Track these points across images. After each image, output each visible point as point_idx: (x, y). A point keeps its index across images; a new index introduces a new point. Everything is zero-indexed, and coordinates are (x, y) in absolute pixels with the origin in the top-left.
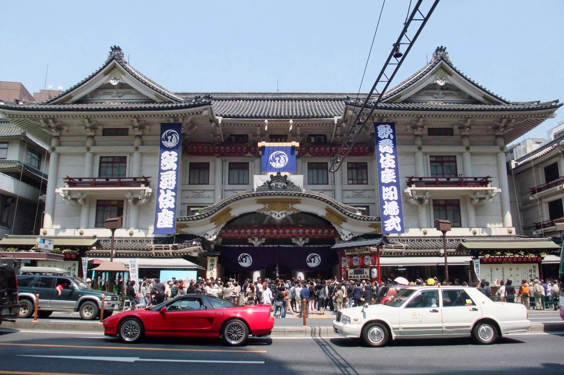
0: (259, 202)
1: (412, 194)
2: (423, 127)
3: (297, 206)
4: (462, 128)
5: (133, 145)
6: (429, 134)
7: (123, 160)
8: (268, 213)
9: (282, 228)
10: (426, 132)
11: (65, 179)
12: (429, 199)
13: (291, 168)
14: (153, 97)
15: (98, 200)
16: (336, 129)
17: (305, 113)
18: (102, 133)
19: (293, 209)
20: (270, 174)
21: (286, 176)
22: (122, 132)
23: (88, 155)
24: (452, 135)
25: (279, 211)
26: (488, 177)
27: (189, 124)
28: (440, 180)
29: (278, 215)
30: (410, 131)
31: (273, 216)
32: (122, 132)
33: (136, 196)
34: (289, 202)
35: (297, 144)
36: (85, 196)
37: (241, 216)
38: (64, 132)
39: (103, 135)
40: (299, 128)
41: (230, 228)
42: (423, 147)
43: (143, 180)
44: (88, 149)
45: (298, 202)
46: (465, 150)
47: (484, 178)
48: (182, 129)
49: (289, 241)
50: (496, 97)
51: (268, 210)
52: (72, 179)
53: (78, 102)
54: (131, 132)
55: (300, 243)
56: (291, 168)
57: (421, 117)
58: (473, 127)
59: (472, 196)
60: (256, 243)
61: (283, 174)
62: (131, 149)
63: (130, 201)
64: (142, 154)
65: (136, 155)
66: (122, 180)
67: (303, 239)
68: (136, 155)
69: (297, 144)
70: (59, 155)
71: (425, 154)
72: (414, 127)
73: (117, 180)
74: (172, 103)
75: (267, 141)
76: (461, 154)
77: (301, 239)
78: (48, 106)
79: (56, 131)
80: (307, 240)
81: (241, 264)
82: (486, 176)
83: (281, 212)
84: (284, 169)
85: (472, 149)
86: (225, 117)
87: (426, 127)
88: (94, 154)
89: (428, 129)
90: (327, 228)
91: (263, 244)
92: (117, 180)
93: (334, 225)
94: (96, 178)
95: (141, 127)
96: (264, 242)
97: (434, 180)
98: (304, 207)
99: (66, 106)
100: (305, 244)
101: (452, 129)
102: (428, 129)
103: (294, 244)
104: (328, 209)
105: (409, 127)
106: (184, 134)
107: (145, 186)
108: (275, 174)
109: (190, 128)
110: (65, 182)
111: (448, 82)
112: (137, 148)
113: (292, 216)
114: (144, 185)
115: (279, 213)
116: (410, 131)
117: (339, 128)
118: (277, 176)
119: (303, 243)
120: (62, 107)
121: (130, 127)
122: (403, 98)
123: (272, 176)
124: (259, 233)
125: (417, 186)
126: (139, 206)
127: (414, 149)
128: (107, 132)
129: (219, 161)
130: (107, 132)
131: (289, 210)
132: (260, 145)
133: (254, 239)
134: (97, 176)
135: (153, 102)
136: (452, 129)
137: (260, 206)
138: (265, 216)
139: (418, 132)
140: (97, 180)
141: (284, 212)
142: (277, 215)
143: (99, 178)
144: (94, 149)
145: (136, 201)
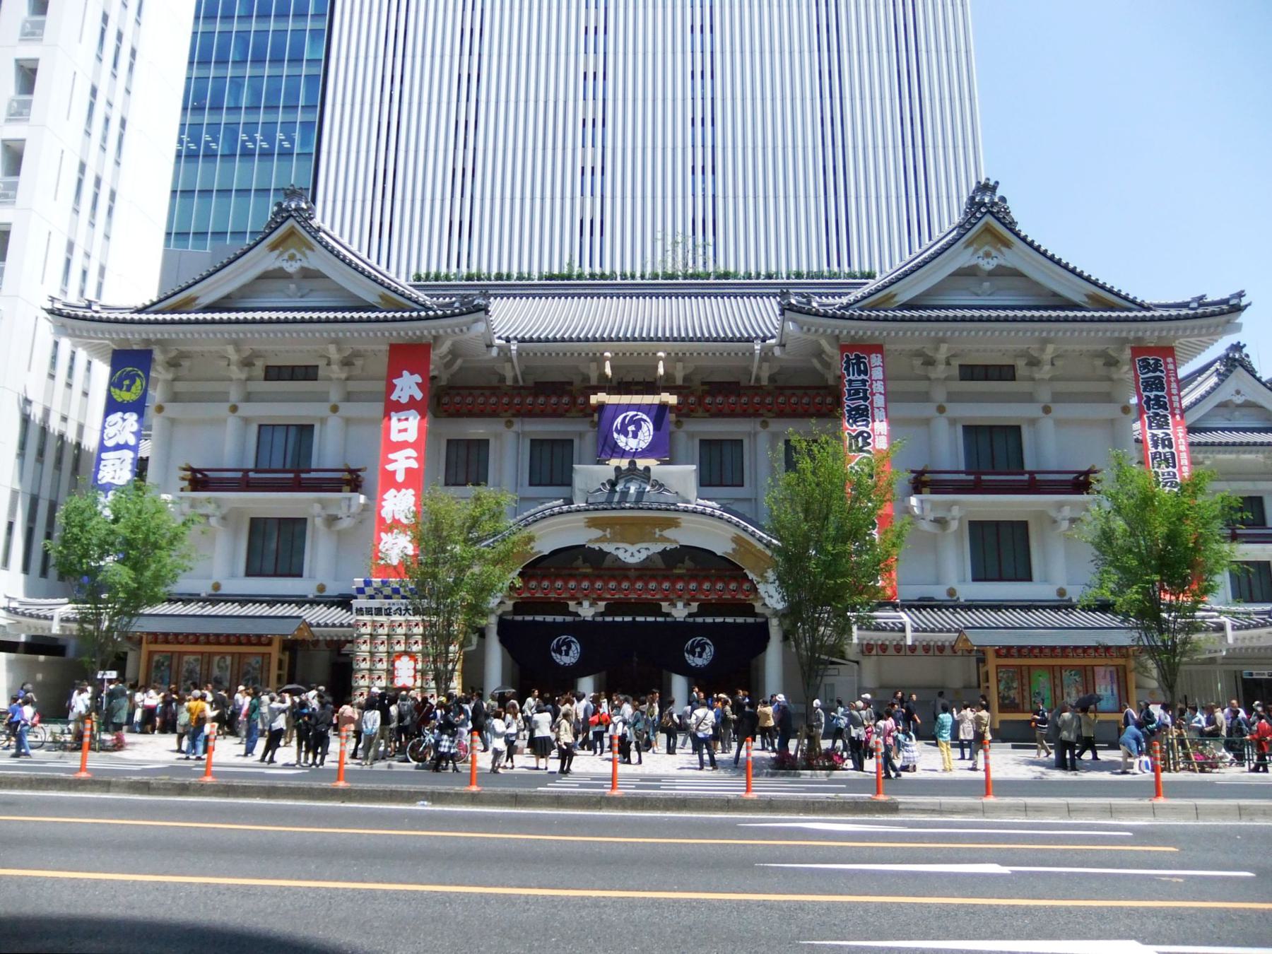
0: (593, 523)
1: (922, 509)
2: (948, 363)
3: (668, 533)
4: (1034, 363)
5: (327, 400)
6: (963, 378)
7: (305, 431)
8: (607, 548)
9: (639, 578)
10: (956, 372)
11: (185, 470)
12: (961, 519)
13: (661, 449)
14: (372, 299)
15: (252, 519)
16: (760, 368)
17: (695, 334)
18: (263, 375)
19: (664, 539)
20: (614, 462)
21: (647, 469)
22: (308, 373)
23: (232, 423)
24: (1013, 378)
25: (633, 544)
26: (1087, 473)
27: (445, 356)
28: (984, 477)
29: (632, 554)
30: (919, 370)
31: (621, 554)
32: (308, 373)
33: (333, 511)
35: (672, 399)
36: (224, 511)
37: (555, 553)
38: (183, 372)
39: (266, 379)
40: (679, 365)
41: (532, 577)
42: (948, 406)
43: (346, 475)
44: (234, 409)
45: (673, 523)
46: (1041, 414)
47: (1081, 473)
48: (432, 367)
49: (655, 609)
50: (1118, 294)
51: (610, 541)
52: (200, 471)
53: (206, 309)
54: (321, 373)
55: (680, 612)
56: (661, 449)
57: (943, 340)
58: (1059, 363)
59: (1053, 513)
60: (587, 611)
61: (641, 463)
62: (320, 409)
63: (319, 522)
64: (348, 421)
65: (334, 422)
67: (687, 604)
68: (334, 422)
69: (672, 399)
70: (173, 422)
71: (953, 422)
72: (930, 362)
73: (291, 475)
74: (412, 310)
76: (1033, 422)
77: (680, 605)
78: (144, 317)
79: (167, 371)
80: (694, 607)
81: (555, 656)
82: (1085, 468)
83: (638, 546)
84: (644, 453)
85: (1061, 410)
86: (523, 340)
87: (956, 363)
88: (246, 421)
89: (961, 366)
90: (734, 579)
91: (602, 614)
92: (291, 475)
93: (751, 576)
94: (247, 471)
95: (347, 363)
96: (602, 609)
97: (972, 477)
98: (689, 534)
99: (184, 317)
100: (690, 615)
101: (1012, 367)
102: (961, 366)
103: (668, 615)
104: (737, 540)
105: (917, 362)
106: (434, 378)
107: (352, 491)
108: (624, 463)
109: (448, 365)
110: (183, 479)
111: (1003, 262)
112: (335, 409)
113: (664, 553)
114: (348, 488)
115: (632, 549)
116: (919, 370)
117: (766, 365)
118: (628, 470)
119: (686, 612)
120: (176, 317)
121: (321, 363)
122: (905, 297)
123: (618, 469)
124: (593, 590)
125: (932, 493)
126: (339, 533)
127: (928, 410)
128: (274, 373)
129: (509, 436)
130: (274, 373)
131: (656, 541)
132: (594, 399)
133: (580, 604)
134: (251, 465)
135: (373, 308)
136: (1013, 367)
137: (597, 533)
138: (602, 554)
139: (940, 371)
140: (252, 475)
141: (645, 545)
142: (628, 554)
143: (256, 471)
144: (247, 409)
145: (332, 520)
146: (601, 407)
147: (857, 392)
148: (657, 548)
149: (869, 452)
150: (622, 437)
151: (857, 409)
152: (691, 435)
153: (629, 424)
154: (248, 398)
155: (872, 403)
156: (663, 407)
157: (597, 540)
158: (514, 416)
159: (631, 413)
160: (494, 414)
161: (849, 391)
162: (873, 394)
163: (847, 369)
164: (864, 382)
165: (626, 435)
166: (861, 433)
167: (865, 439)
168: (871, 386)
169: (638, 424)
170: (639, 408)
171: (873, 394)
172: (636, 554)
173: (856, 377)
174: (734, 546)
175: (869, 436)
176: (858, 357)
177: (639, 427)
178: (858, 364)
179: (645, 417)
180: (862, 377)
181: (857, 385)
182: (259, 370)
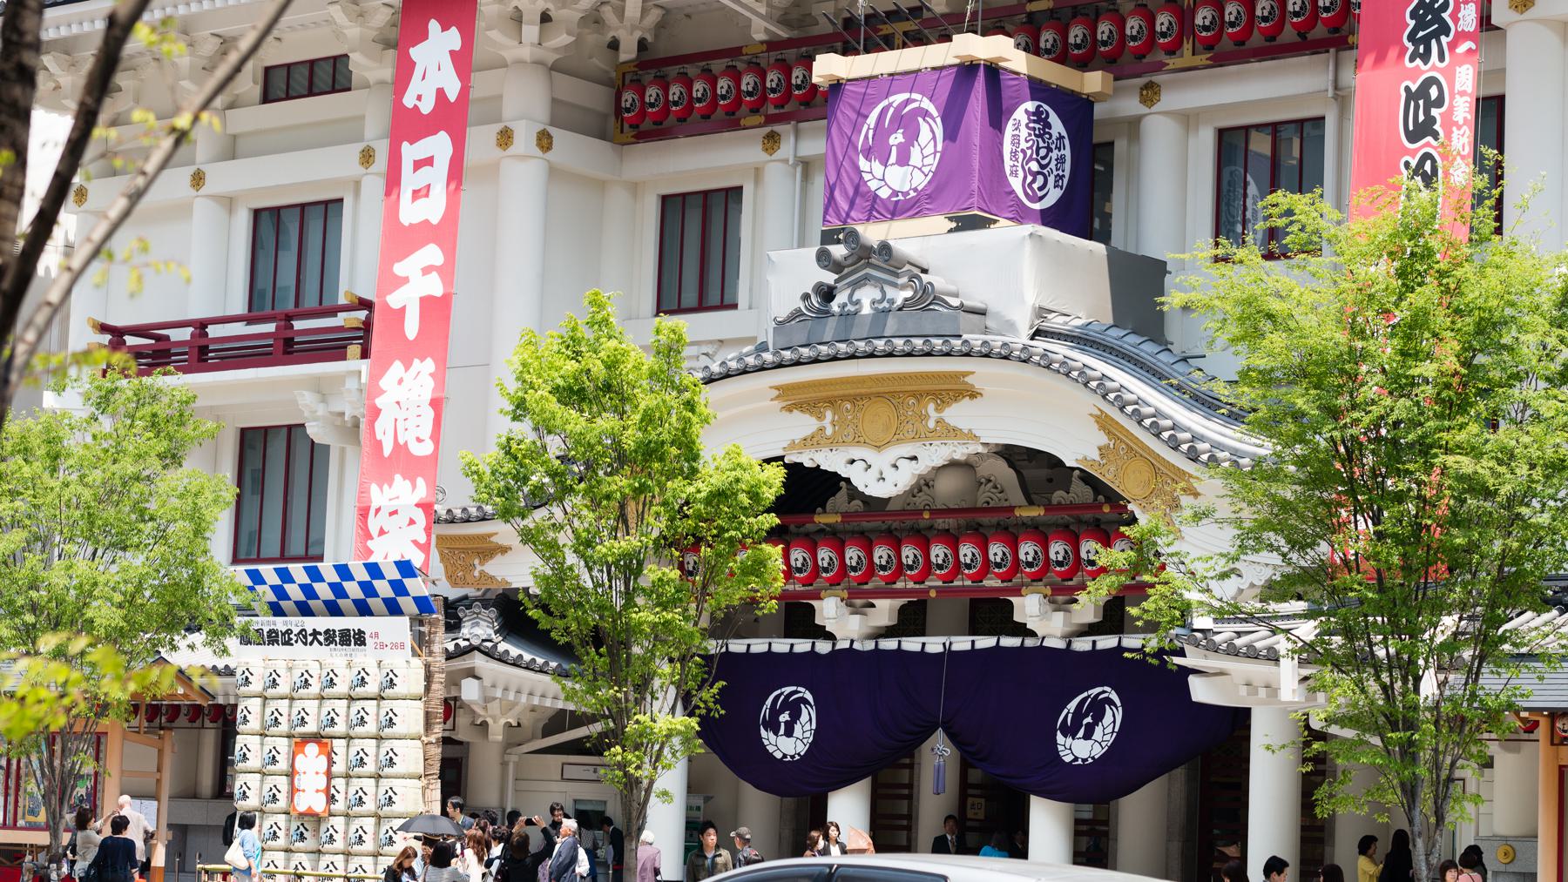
18: (257, 91)
19: (953, 433)
23: (203, 210)
34: (919, 396)
39: (266, 99)
45: (957, 390)
51: (833, 443)
66: (299, 325)
75: (847, 51)
88: (229, 203)
91: (889, 632)
92: (270, 327)
94: (201, 325)
130: (282, 84)
140: (214, 331)
143: (249, 320)
144: (227, 177)
146: (837, 87)
148: (934, 455)
150: (877, 167)
152: (1188, 120)
154: (232, 149)
156: (967, 70)
157: (809, 442)
158: (770, 119)
160: (732, 123)
169: (907, 121)
170: (910, 79)
172: (889, 473)
174: (1103, 439)
182: (249, 84)
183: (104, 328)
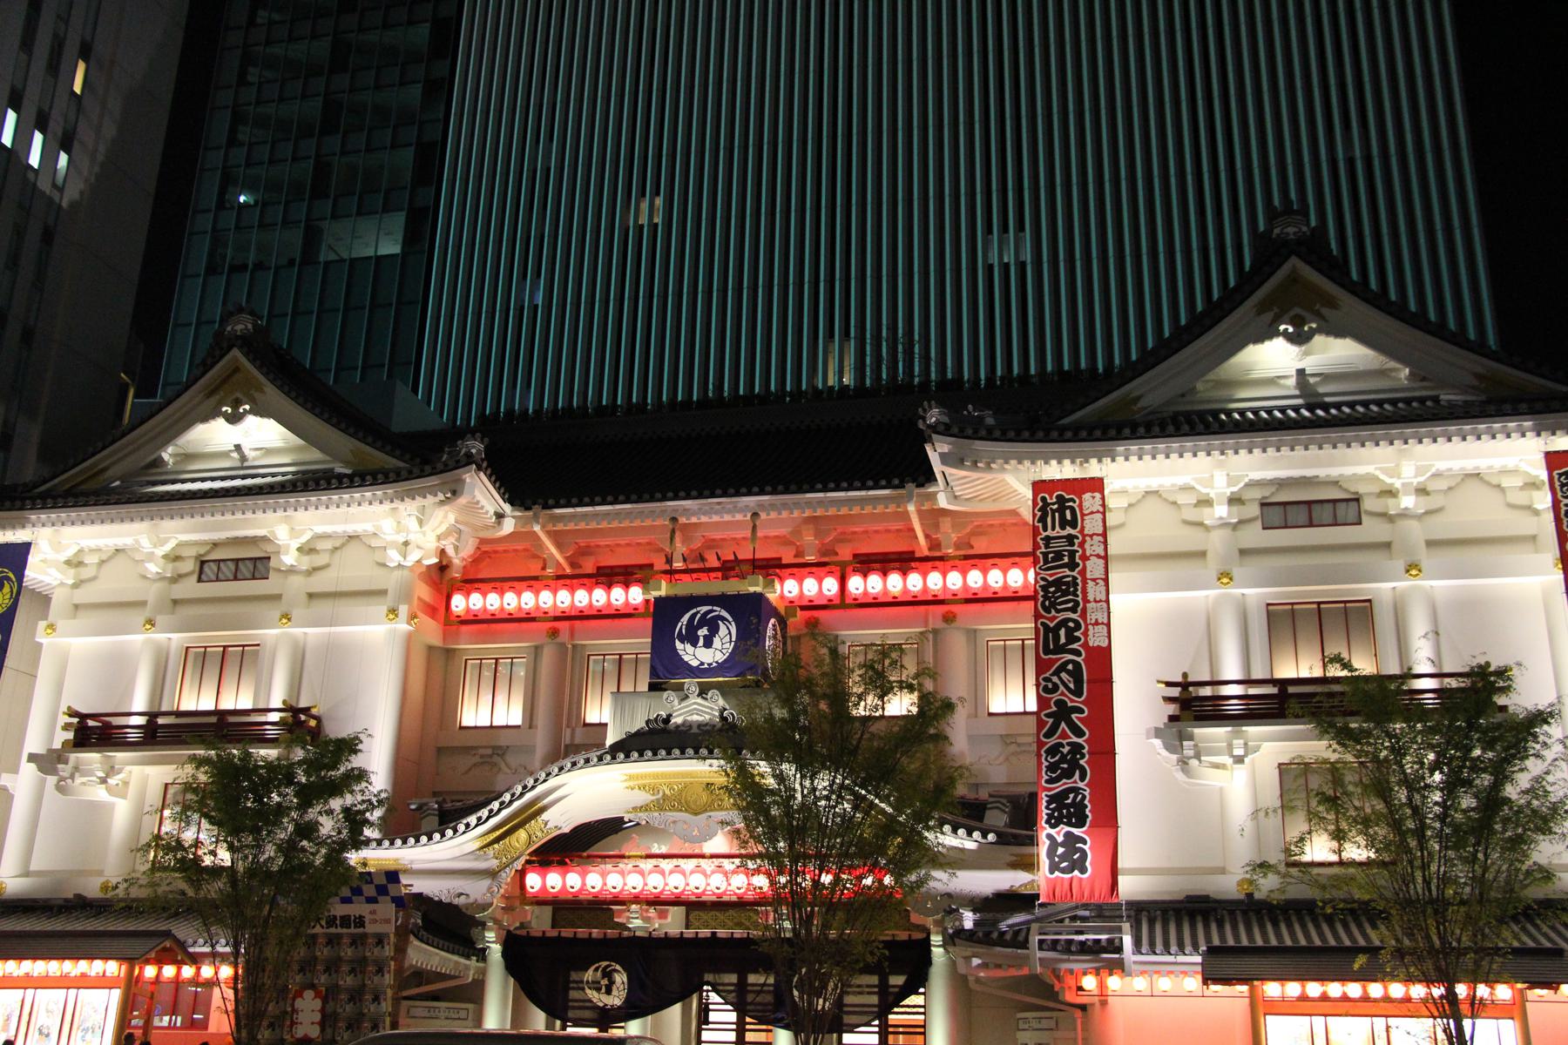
147: (1059, 555)
149: (1078, 653)
151: (1058, 582)
153: (700, 626)
155: (1083, 572)
159: (704, 609)
161: (1045, 555)
162: (1085, 558)
163: (1043, 520)
164: (1070, 539)
165: (695, 644)
166: (1064, 622)
167: (1070, 632)
168: (1082, 545)
171: (1085, 558)
173: (1058, 532)
175: (1078, 627)
176: (1061, 499)
177: (714, 630)
178: (1061, 510)
179: (724, 614)
180: (1069, 531)
181: (1056, 546)
183: (72, 713)
